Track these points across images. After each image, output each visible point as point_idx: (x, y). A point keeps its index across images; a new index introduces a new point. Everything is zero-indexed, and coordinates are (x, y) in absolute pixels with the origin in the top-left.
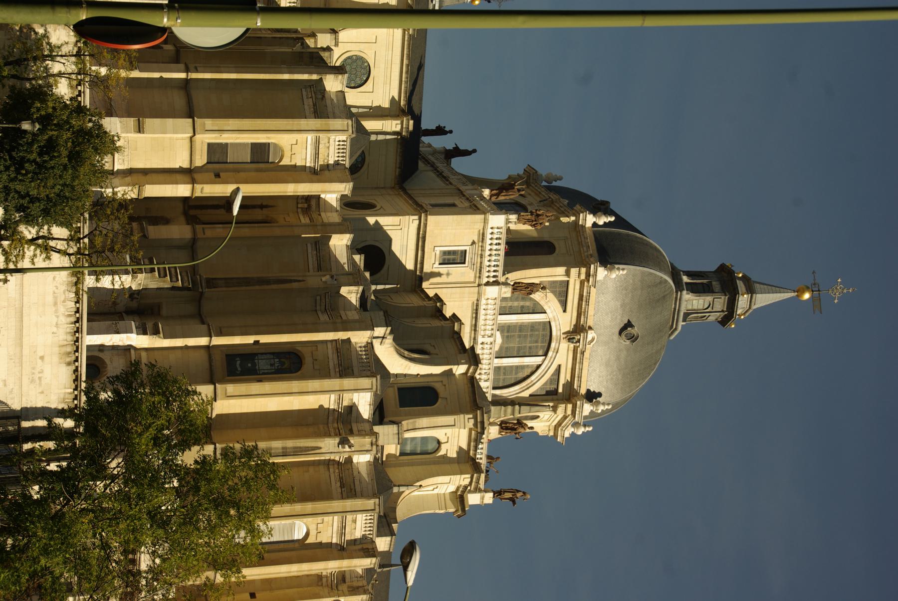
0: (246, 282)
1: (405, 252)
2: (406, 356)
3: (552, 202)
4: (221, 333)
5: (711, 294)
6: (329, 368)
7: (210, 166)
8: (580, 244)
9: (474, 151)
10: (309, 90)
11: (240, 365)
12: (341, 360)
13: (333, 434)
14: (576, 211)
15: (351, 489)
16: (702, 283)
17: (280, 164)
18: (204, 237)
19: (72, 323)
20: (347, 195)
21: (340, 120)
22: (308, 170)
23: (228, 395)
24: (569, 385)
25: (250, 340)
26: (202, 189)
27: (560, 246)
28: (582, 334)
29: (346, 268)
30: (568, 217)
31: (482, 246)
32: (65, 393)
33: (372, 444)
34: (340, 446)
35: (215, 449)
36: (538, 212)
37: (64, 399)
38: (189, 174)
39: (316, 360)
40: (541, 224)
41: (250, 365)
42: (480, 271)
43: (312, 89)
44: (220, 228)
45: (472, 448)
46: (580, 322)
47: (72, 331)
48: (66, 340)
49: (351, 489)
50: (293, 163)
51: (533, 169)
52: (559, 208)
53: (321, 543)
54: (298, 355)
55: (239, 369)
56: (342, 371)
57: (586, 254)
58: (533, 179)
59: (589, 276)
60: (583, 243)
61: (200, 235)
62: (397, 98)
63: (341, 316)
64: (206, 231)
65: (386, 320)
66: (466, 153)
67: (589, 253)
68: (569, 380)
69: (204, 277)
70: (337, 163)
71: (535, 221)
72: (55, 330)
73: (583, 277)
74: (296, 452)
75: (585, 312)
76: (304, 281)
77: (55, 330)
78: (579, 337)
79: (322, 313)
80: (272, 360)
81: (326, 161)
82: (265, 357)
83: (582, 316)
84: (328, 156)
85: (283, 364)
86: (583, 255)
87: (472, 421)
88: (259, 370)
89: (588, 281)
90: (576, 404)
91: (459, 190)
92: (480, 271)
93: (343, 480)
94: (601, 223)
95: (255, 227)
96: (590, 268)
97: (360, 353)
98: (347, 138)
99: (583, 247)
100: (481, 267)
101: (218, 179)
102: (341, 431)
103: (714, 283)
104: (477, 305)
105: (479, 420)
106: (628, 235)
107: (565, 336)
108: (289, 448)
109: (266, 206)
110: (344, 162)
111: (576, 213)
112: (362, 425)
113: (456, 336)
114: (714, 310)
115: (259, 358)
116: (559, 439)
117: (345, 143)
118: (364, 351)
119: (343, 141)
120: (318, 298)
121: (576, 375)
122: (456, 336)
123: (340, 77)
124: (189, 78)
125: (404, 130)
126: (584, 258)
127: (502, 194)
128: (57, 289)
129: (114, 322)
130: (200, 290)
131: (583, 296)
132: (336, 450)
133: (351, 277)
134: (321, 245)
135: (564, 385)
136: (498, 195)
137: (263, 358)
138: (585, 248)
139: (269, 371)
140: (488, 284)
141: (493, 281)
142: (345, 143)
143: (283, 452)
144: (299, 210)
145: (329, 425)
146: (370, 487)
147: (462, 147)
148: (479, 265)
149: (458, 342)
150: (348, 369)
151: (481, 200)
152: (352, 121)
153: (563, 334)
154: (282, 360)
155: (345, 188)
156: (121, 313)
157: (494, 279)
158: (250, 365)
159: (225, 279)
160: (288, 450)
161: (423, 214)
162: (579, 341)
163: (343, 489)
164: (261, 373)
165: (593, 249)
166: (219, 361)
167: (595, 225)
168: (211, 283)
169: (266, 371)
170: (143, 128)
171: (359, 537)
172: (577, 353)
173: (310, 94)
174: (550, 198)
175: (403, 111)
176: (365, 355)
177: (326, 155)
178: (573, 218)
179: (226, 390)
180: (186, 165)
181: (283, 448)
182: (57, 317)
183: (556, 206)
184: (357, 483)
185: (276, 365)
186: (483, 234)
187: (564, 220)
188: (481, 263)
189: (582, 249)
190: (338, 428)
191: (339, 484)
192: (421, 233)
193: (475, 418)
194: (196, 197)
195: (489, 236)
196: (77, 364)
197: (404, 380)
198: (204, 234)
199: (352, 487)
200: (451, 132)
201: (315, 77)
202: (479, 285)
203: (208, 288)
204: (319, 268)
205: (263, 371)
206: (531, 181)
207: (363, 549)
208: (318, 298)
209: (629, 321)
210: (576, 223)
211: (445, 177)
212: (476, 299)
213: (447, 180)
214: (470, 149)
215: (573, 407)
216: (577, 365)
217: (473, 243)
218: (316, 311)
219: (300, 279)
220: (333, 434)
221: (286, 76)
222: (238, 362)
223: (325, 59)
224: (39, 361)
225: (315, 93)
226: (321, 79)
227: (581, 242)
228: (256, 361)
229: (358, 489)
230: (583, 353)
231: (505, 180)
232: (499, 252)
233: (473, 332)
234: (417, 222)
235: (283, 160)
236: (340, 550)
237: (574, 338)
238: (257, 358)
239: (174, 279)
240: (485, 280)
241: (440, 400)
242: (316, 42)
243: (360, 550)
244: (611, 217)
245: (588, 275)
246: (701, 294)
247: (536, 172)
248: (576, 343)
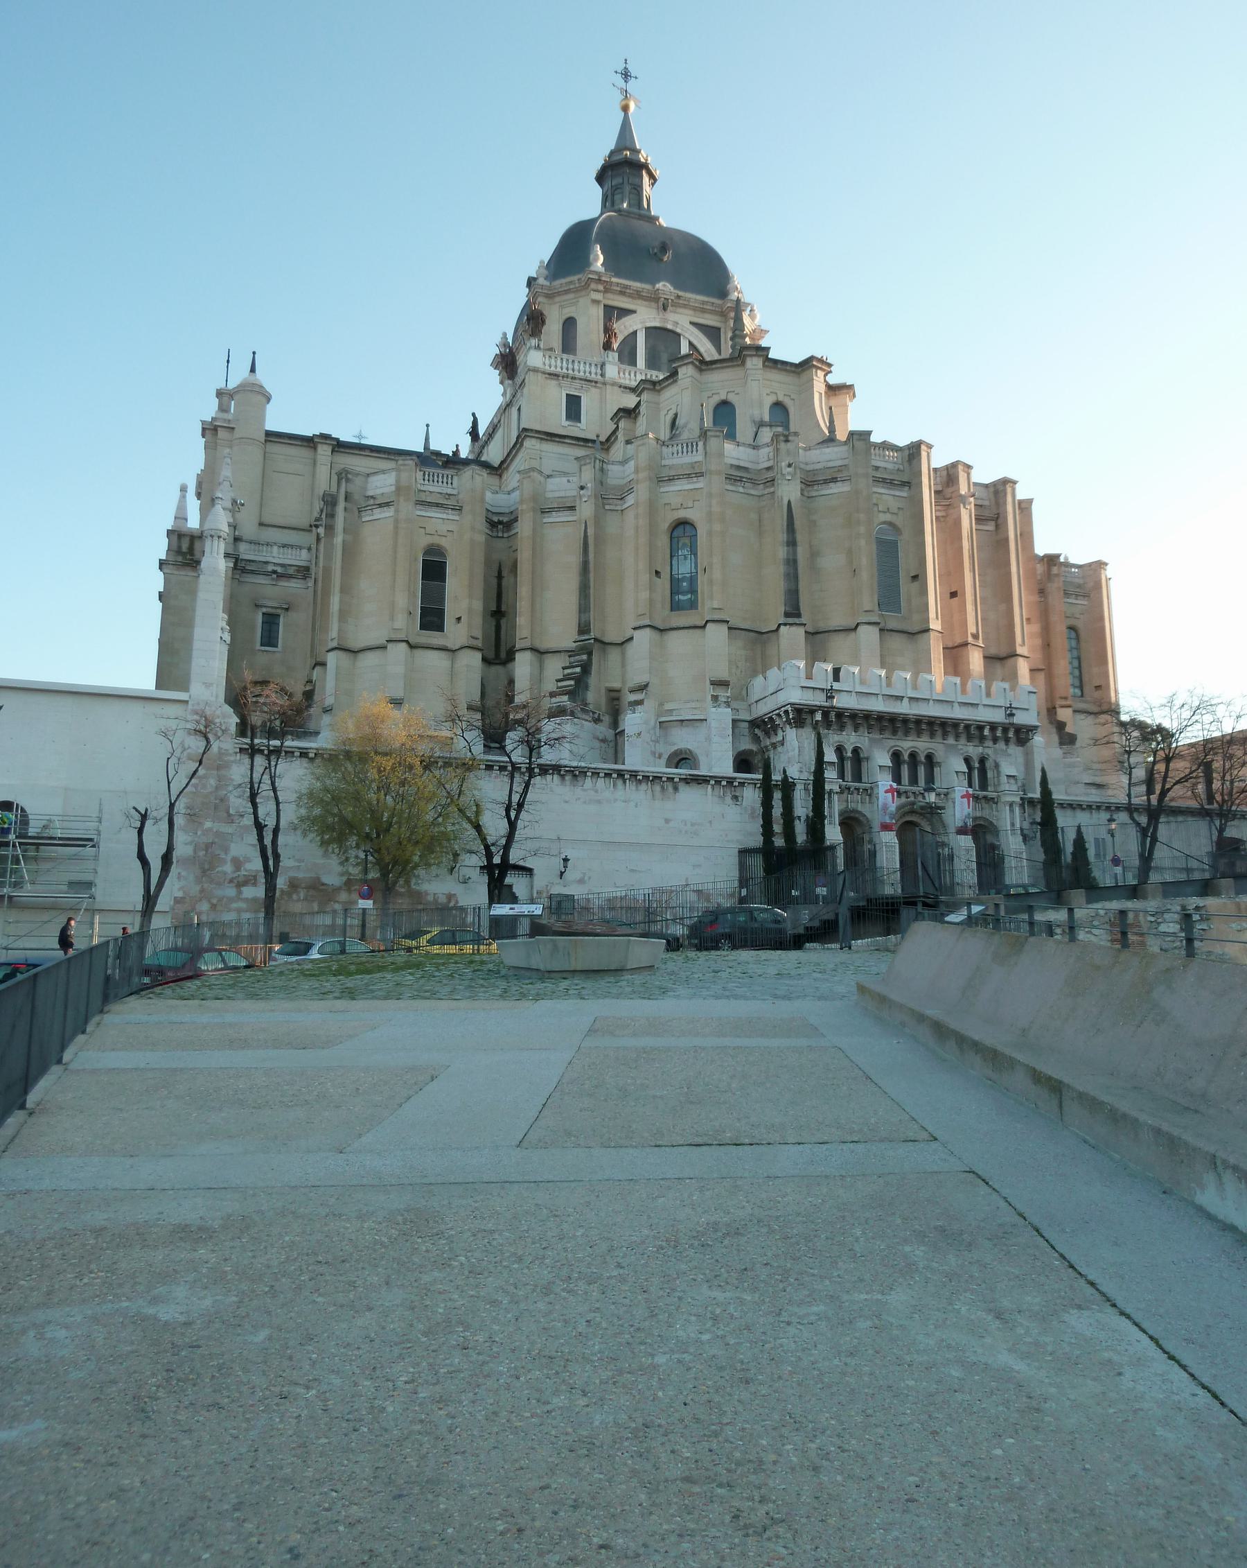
9: (474, 415)
10: (363, 514)
13: (772, 490)
27: (569, 312)
35: (785, 624)
37: (720, 797)
49: (838, 471)
55: (689, 596)
61: (527, 644)
72: (632, 804)
77: (632, 804)
82: (675, 567)
84: (441, 493)
91: (505, 409)
98: (420, 471)
107: (661, 314)
109: (500, 572)
117: (427, 473)
119: (424, 475)
128: (579, 799)
129: (626, 739)
130: (592, 641)
133: (583, 468)
142: (427, 473)
144: (506, 535)
148: (583, 382)
155: (479, 475)
156: (616, 734)
158: (685, 584)
168: (584, 629)
169: (693, 565)
182: (616, 800)
191: (832, 485)
195: (553, 368)
199: (836, 469)
200: (457, 446)
204: (572, 508)
208: (607, 507)
211: (494, 430)
224: (672, 824)
229: (839, 463)
240: (599, 377)
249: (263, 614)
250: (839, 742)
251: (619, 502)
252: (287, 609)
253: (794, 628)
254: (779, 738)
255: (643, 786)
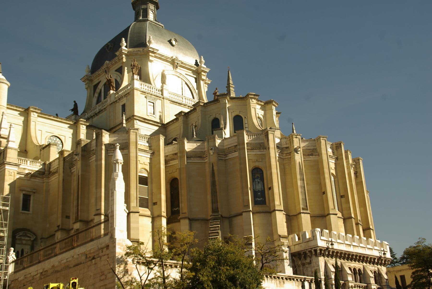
0: (214, 193)
1: (149, 129)
2: (224, 126)
3: (107, 67)
4: (247, 206)
5: (148, 9)
6: (261, 154)
7: (150, 207)
8: (136, 55)
9: (75, 102)
10: (109, 152)
11: (259, 198)
12: (257, 148)
13: (289, 157)
14: (119, 54)
15: (313, 151)
16: (142, 12)
17: (149, 171)
18: (187, 213)
19: (267, 279)
20: (164, 139)
21: (130, 135)
22: (152, 157)
23: (280, 204)
24: (193, 72)
25: (249, 191)
26: (163, 212)
28: (175, 61)
29: (199, 144)
30: (123, 58)
31: (147, 94)
32: (295, 285)
33: (296, 138)
34: (298, 153)
35: (303, 213)
36: (133, 65)
37: (298, 286)
38: (155, 218)
39: (257, 160)
40: (138, 65)
41: (259, 194)
42: (157, 97)
43: (109, 150)
44: (181, 205)
45: (261, 103)
46: (170, 61)
47: (270, 280)
48: (274, 283)
50: (148, 164)
51: (83, 77)
52: (112, 65)
53: (335, 168)
54: (254, 169)
55: (261, 199)
56: (263, 148)
57: (142, 52)
58: (89, 78)
59: (153, 52)
60: (136, 53)
61: (186, 215)
62: (69, 125)
63: (228, 148)
64: (184, 212)
65: (218, 130)
66: (76, 105)
67: (142, 51)
68: (191, 72)
69: (211, 214)
70: (148, 142)
71: (137, 67)
73: (153, 55)
74: (302, 174)
75: (166, 58)
76: (212, 164)
78: (176, 63)
79: (227, 157)
80: (256, 182)
81: (147, 147)
82: (255, 185)
83: (168, 60)
84: (145, 146)
85: (258, 177)
86: (142, 54)
87: (253, 100)
88: (262, 189)
89: (155, 53)
90: (202, 70)
92: (157, 97)
93: (309, 154)
94: (125, 44)
95: (181, 187)
96: (150, 51)
97: (252, 139)
99: (138, 53)
100: (156, 96)
101: (158, 204)
102: (288, 152)
103: (142, 7)
104: (171, 101)
105: (253, 97)
106: (131, 34)
107: (175, 69)
108: (300, 177)
110: (147, 138)
111: (121, 54)
112: (283, 143)
113: (205, 105)
114: (154, 10)
115: (255, 188)
116: (209, 83)
118: (251, 136)
120: (219, 158)
121: (190, 68)
122: (205, 105)
123: (103, 134)
124: (104, 214)
125: (85, 124)
126: (144, 54)
127: (113, 85)
130: (220, 216)
131: (160, 57)
132: (300, 155)
134: (191, 155)
135: (193, 74)
136: (113, 87)
137: (255, 187)
138: (139, 52)
139: (262, 184)
140: (162, 95)
141: (161, 92)
143: (302, 180)
145: (284, 158)
146: (310, 142)
147: (72, 107)
149: (209, 104)
150: (261, 145)
151: (118, 93)
152: (131, 129)
153: (174, 69)
154: (256, 177)
157: (160, 91)
158: (259, 194)
159: (212, 203)
160: (301, 178)
161: (135, 117)
162: (178, 63)
163: (314, 154)
164: (263, 188)
165: (141, 49)
166: (259, 208)
167: (126, 47)
169: (262, 186)
170: (136, 239)
171: (331, 150)
172: (181, 65)
173: (111, 151)
174: (105, 69)
175: (75, 123)
176: (253, 136)
177: (144, 146)
178: (124, 56)
179: (278, 205)
180: (150, 220)
181: (300, 180)
183: (110, 66)
184: (309, 148)
185: (259, 180)
186: (142, 92)
187: (124, 60)
188: (154, 95)
189: (139, 54)
190: (286, 154)
191: (311, 156)
192: (142, 120)
193: (252, 98)
194: (166, 216)
196: (284, 278)
197: (232, 130)
198: (185, 213)
199: (311, 150)
201: (103, 147)
202: (163, 98)
203: (218, 212)
205: (262, 187)
206: (90, 78)
207: (336, 149)
208: (219, 158)
209: (168, 41)
210: (126, 55)
212: (169, 101)
213: (102, 110)
214: (74, 103)
215: (203, 72)
216: (186, 66)
217: (146, 97)
218: (225, 160)
219: (211, 165)
220: (289, 157)
221: (103, 162)
222: (258, 199)
223: (85, 144)
225: (111, 149)
226: (105, 145)
227: (135, 54)
228: (257, 190)
229: (312, 148)
230: (182, 63)
231: (88, 92)
232: (149, 87)
233: (182, 105)
234: (137, 121)
235: (147, 169)
236: (337, 160)
237: (176, 65)
238: (255, 190)
239: (218, 228)
241: (240, 115)
242: (67, 151)
243: (337, 150)
244: (123, 39)
245: (153, 52)
246: (148, 13)
247: (86, 75)
248: (178, 65)
249: (24, 194)
250: (332, 263)
251: (224, 156)
252: (34, 193)
253: (306, 215)
254: (308, 260)
255: (274, 281)
